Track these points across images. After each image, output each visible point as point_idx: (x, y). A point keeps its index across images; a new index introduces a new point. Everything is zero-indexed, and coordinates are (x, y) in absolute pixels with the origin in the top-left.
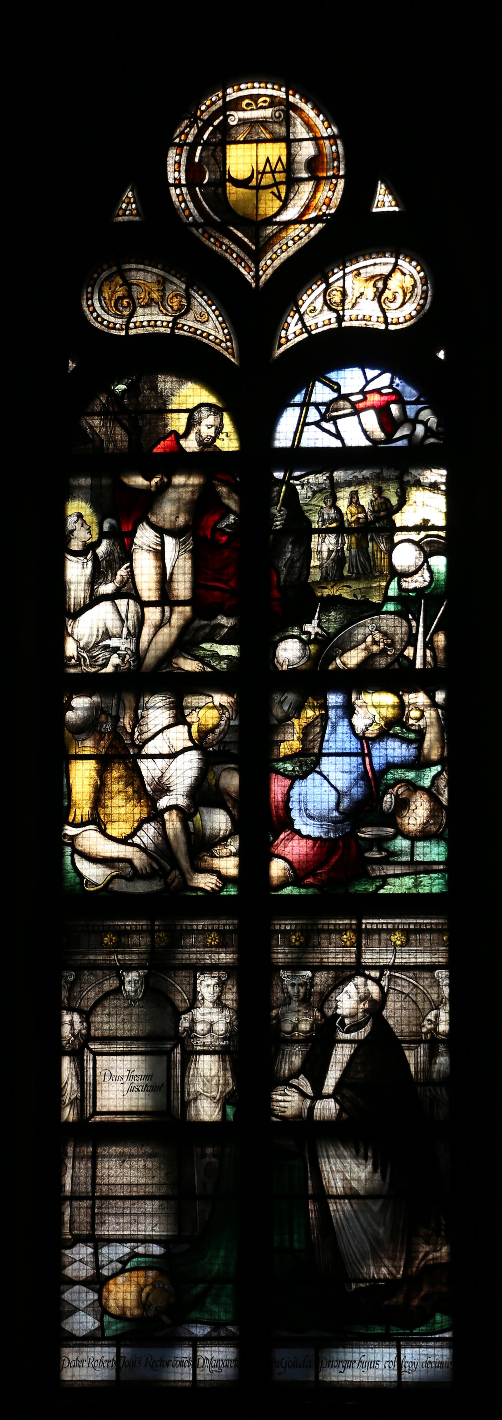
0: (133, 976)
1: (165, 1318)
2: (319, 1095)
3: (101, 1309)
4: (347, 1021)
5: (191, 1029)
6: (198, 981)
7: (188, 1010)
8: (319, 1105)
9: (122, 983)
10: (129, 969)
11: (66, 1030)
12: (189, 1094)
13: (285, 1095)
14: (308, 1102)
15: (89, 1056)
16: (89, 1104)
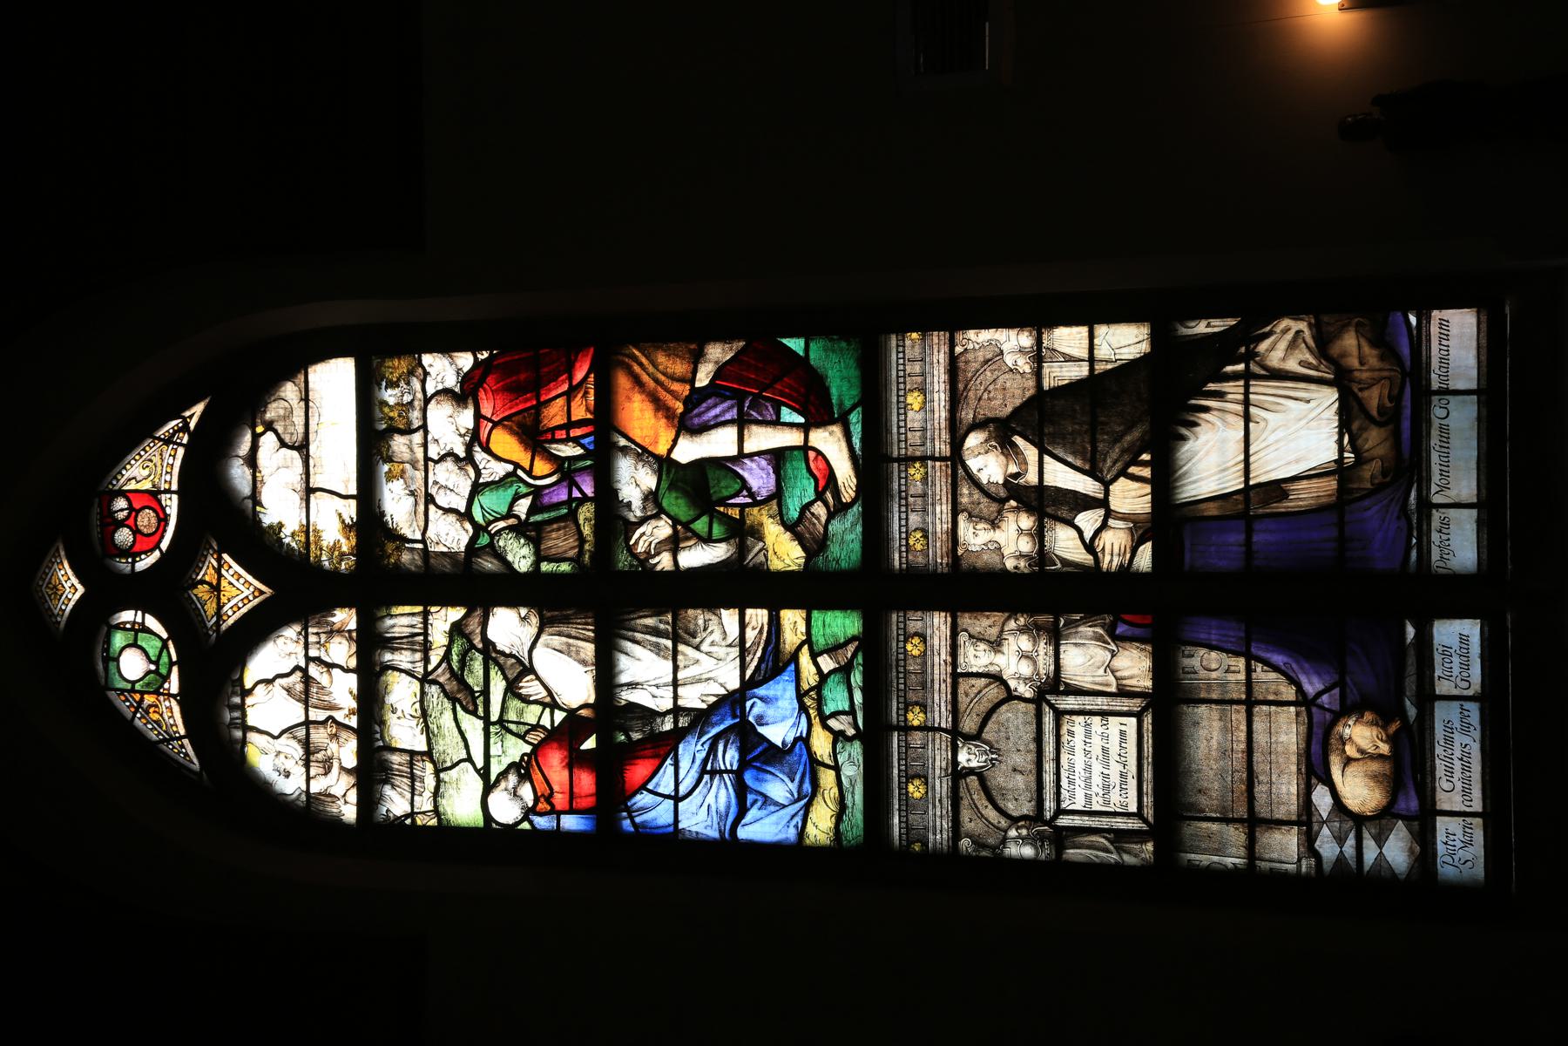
0: (963, 757)
1: (1393, 728)
2: (1103, 503)
3: (1381, 821)
4: (1013, 469)
5: (1026, 680)
7: (1004, 683)
8: (1116, 504)
9: (971, 771)
10: (955, 762)
11: (1028, 851)
12: (1107, 685)
13: (1103, 549)
14: (1111, 522)
15: (1064, 821)
16: (1121, 823)
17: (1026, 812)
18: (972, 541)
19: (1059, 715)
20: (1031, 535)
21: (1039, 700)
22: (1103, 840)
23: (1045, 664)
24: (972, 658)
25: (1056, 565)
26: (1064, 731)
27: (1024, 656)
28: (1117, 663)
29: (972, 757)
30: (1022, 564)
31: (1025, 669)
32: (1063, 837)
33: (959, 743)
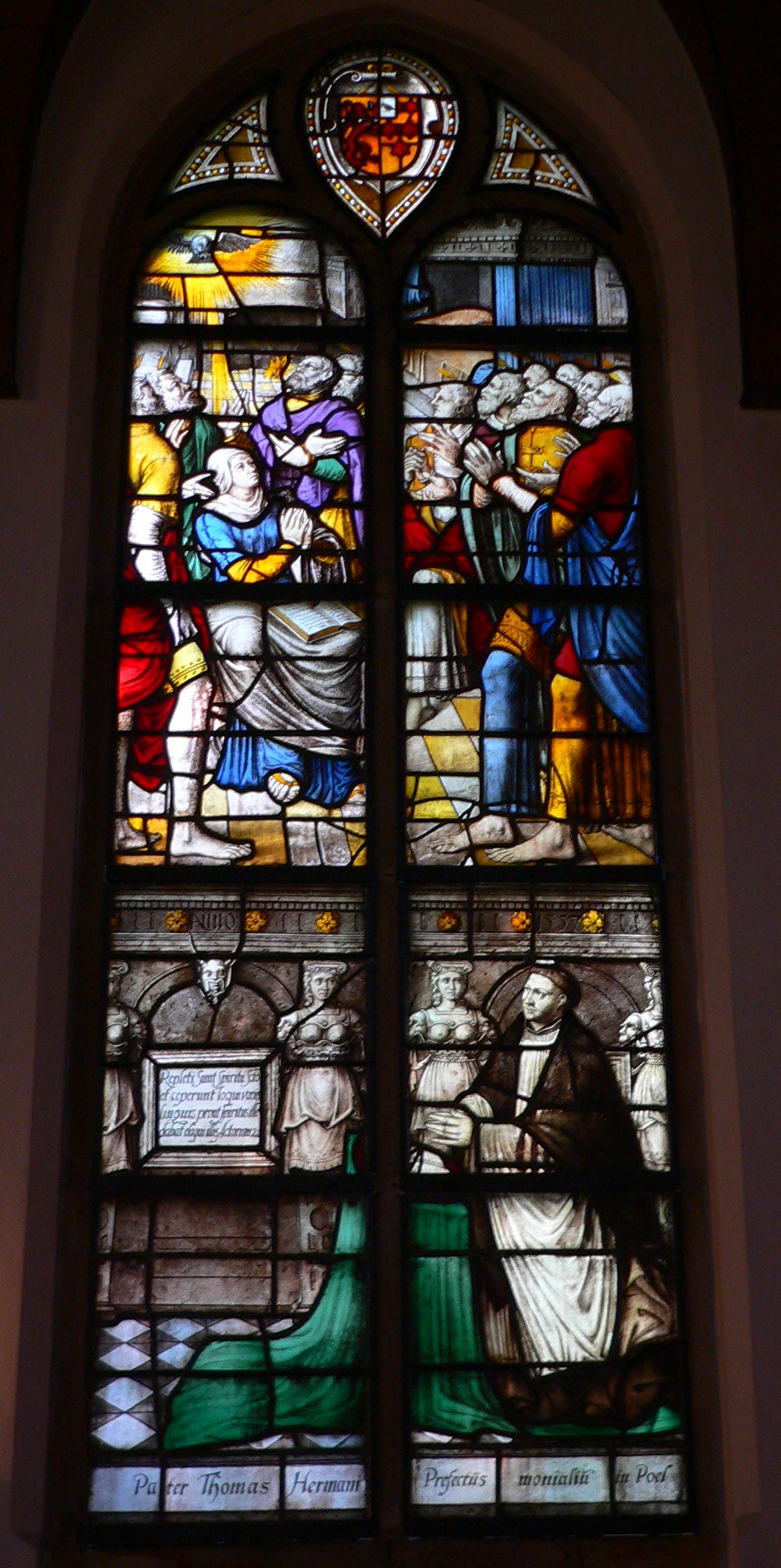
6: (306, 973)
11: (114, 1033)
17: (157, 1031)
18: (442, 977)
19: (262, 1065)
20: (448, 1037)
21: (278, 1048)
22: (127, 1117)
23: (313, 1053)
24: (316, 977)
25: (418, 1061)
26: (244, 1071)
27: (323, 1032)
28: (315, 1129)
29: (214, 976)
30: (415, 1030)
31: (308, 1031)
32: (129, 1069)
33: (229, 961)
